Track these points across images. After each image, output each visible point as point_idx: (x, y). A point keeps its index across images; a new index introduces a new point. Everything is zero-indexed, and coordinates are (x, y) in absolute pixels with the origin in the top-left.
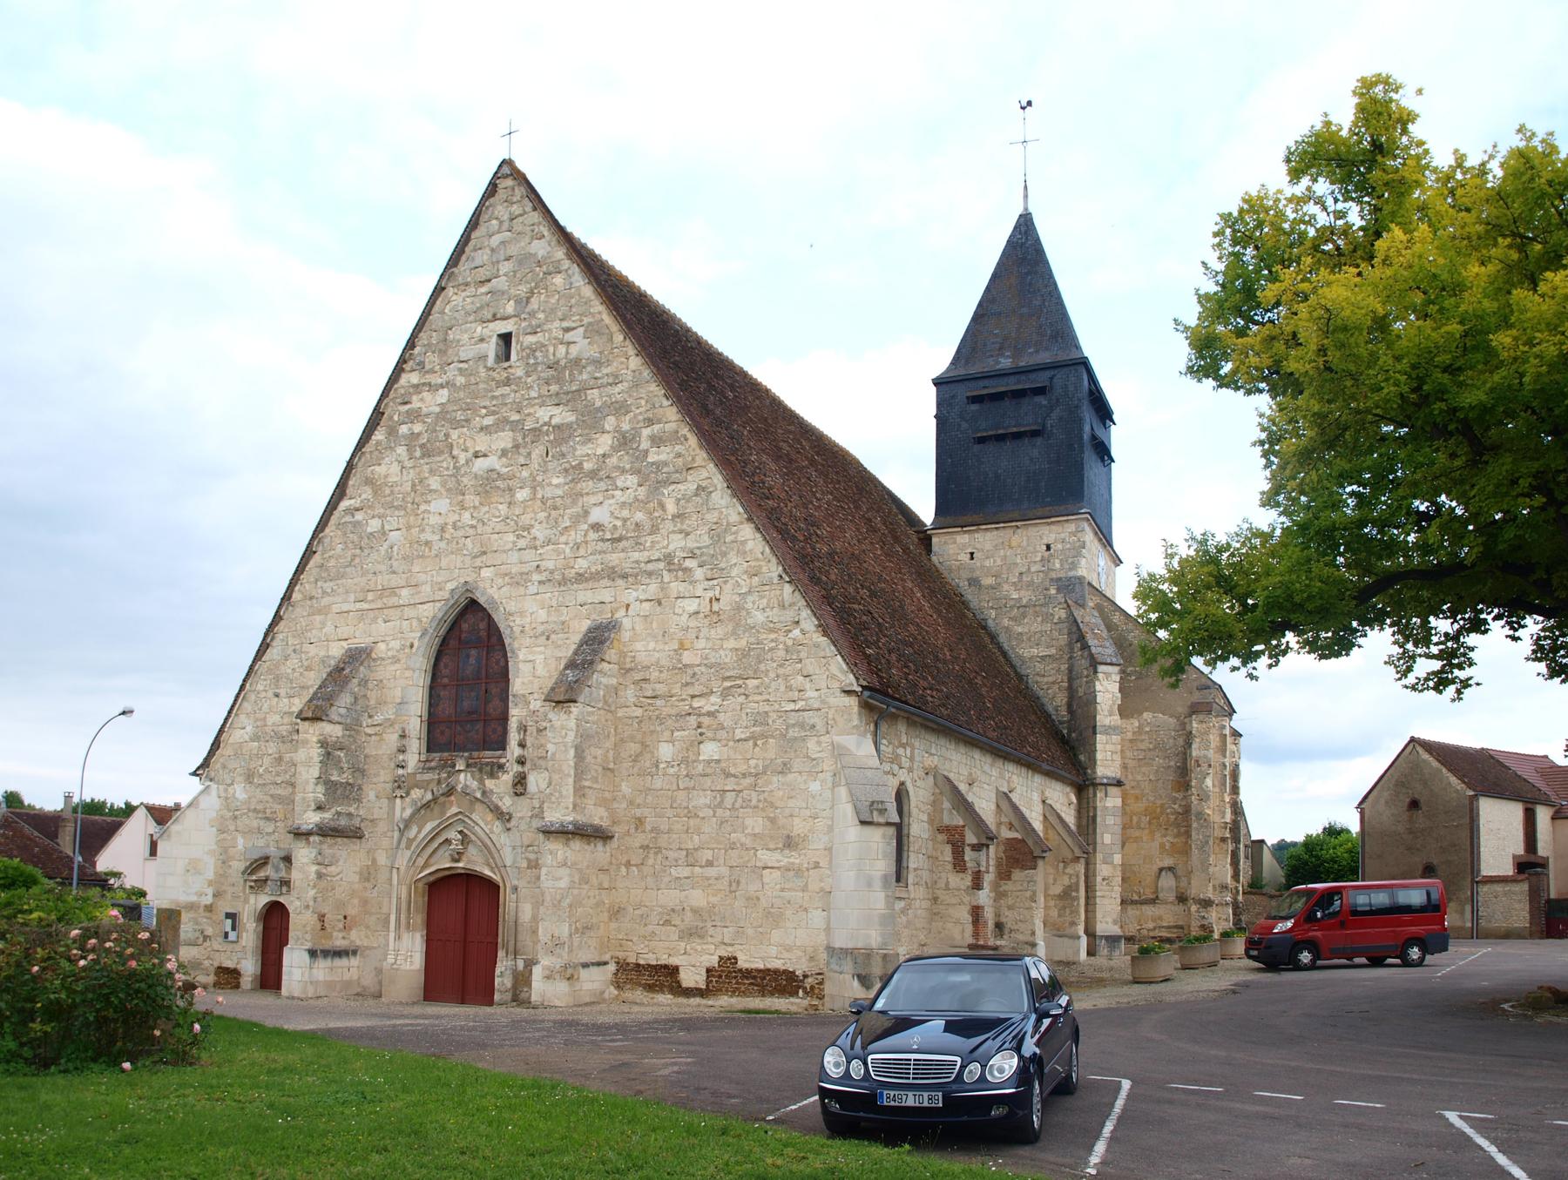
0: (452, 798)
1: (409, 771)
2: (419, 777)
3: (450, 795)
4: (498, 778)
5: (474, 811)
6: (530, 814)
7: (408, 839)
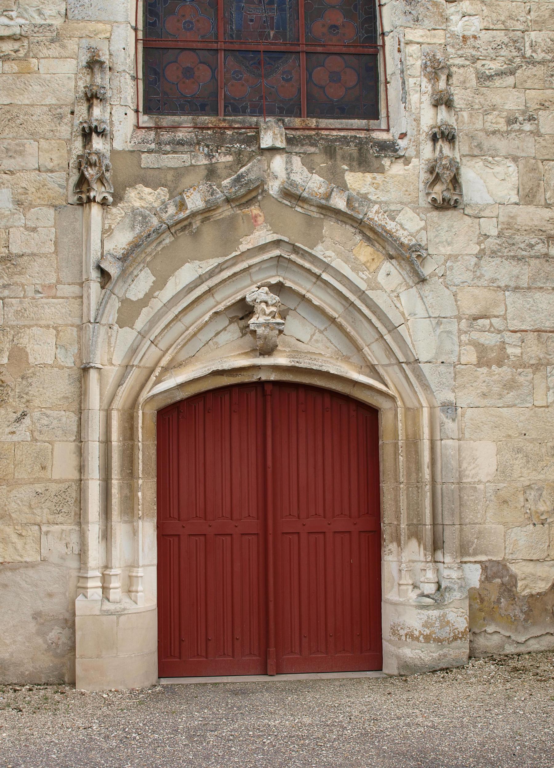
0: (254, 210)
1: (118, 145)
2: (147, 160)
3: (249, 203)
4: (381, 170)
5: (320, 239)
6: (476, 249)
7: (125, 301)
